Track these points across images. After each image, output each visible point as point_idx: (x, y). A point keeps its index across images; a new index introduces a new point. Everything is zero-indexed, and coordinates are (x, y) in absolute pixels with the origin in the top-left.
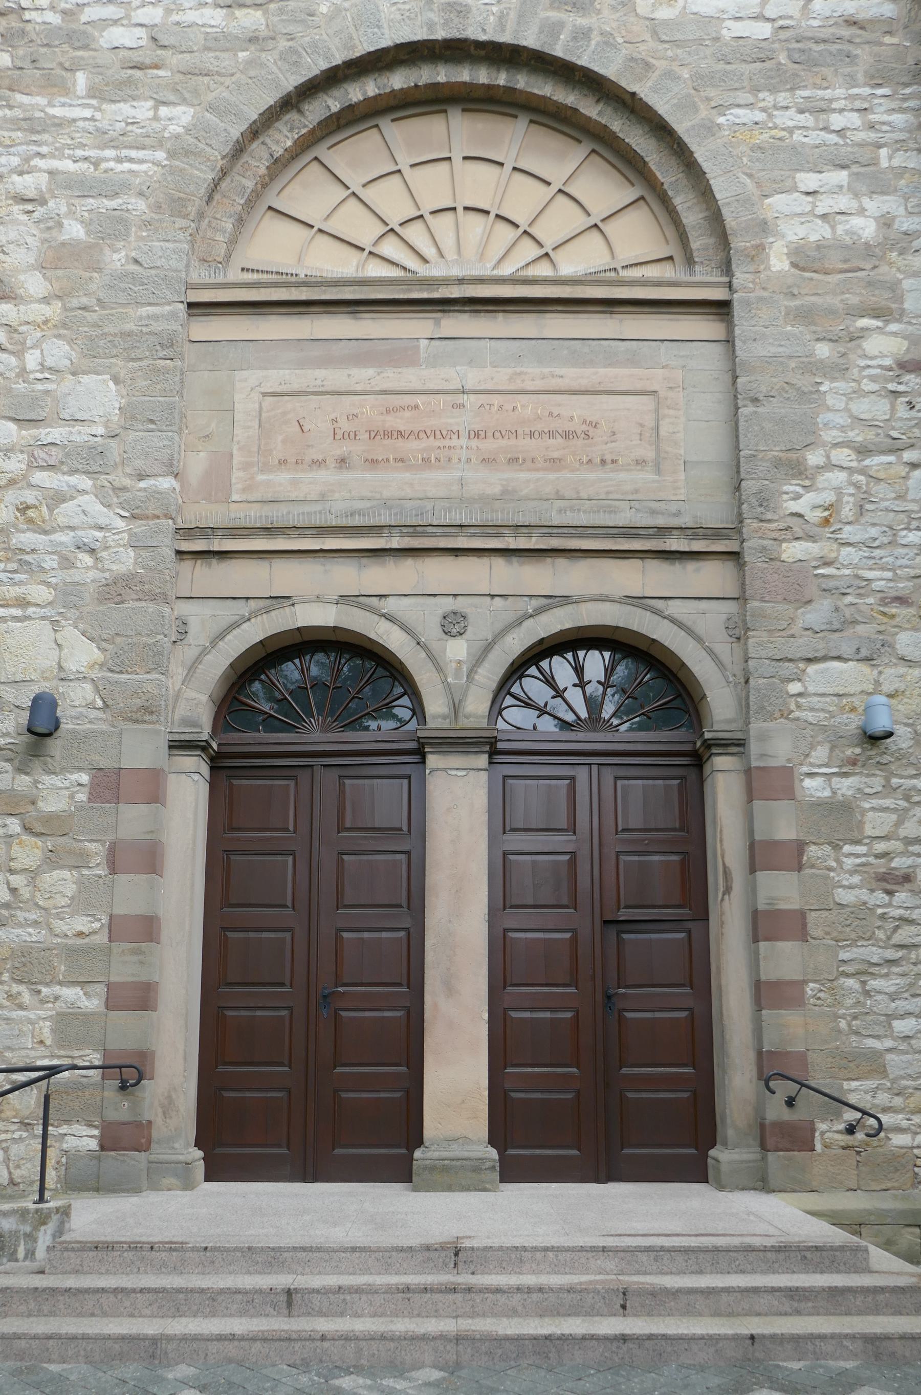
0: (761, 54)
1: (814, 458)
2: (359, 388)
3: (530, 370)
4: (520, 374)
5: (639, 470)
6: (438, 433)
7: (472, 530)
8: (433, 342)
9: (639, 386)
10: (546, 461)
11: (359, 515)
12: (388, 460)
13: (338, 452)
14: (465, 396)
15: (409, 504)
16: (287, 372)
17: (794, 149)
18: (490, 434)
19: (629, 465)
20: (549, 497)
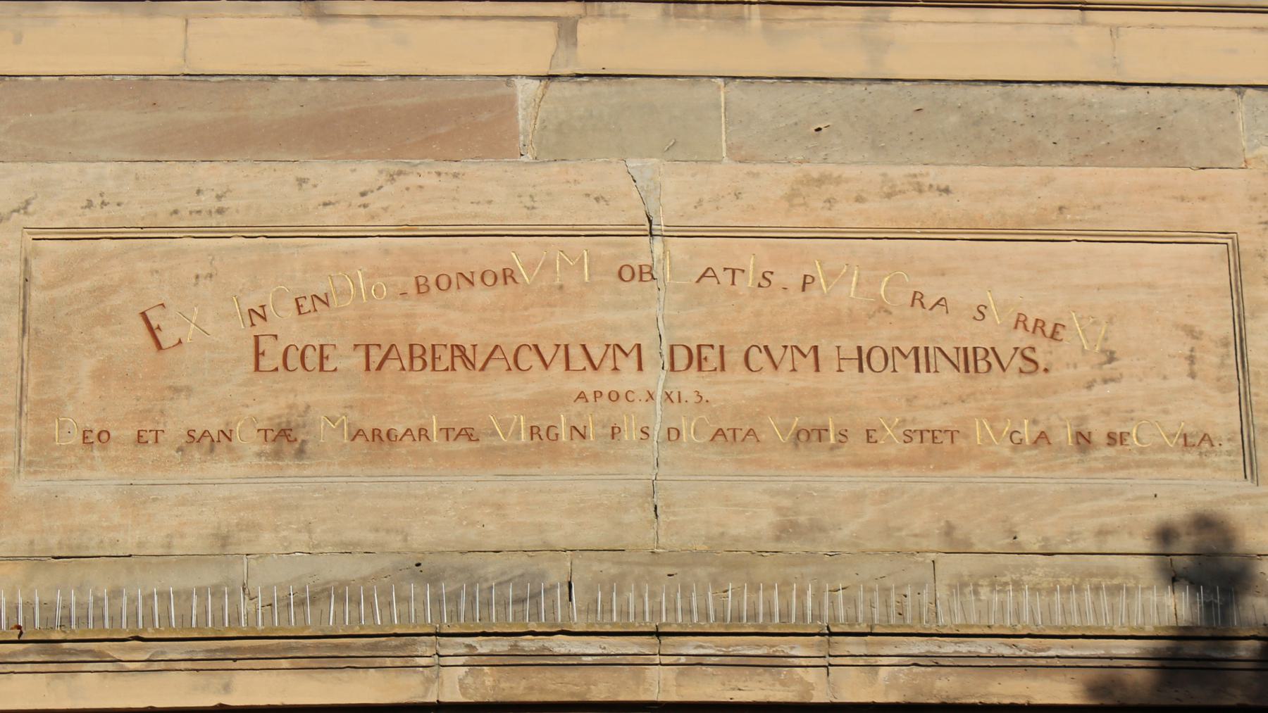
2: (332, 218)
3: (849, 171)
4: (821, 181)
5: (1191, 465)
6: (576, 352)
7: (691, 646)
8: (554, 85)
9: (1177, 216)
10: (908, 437)
11: (340, 599)
12: (423, 433)
13: (270, 403)
14: (658, 244)
15: (493, 567)
16: (110, 168)
18: (734, 357)
19: (1163, 448)
20: (925, 544)
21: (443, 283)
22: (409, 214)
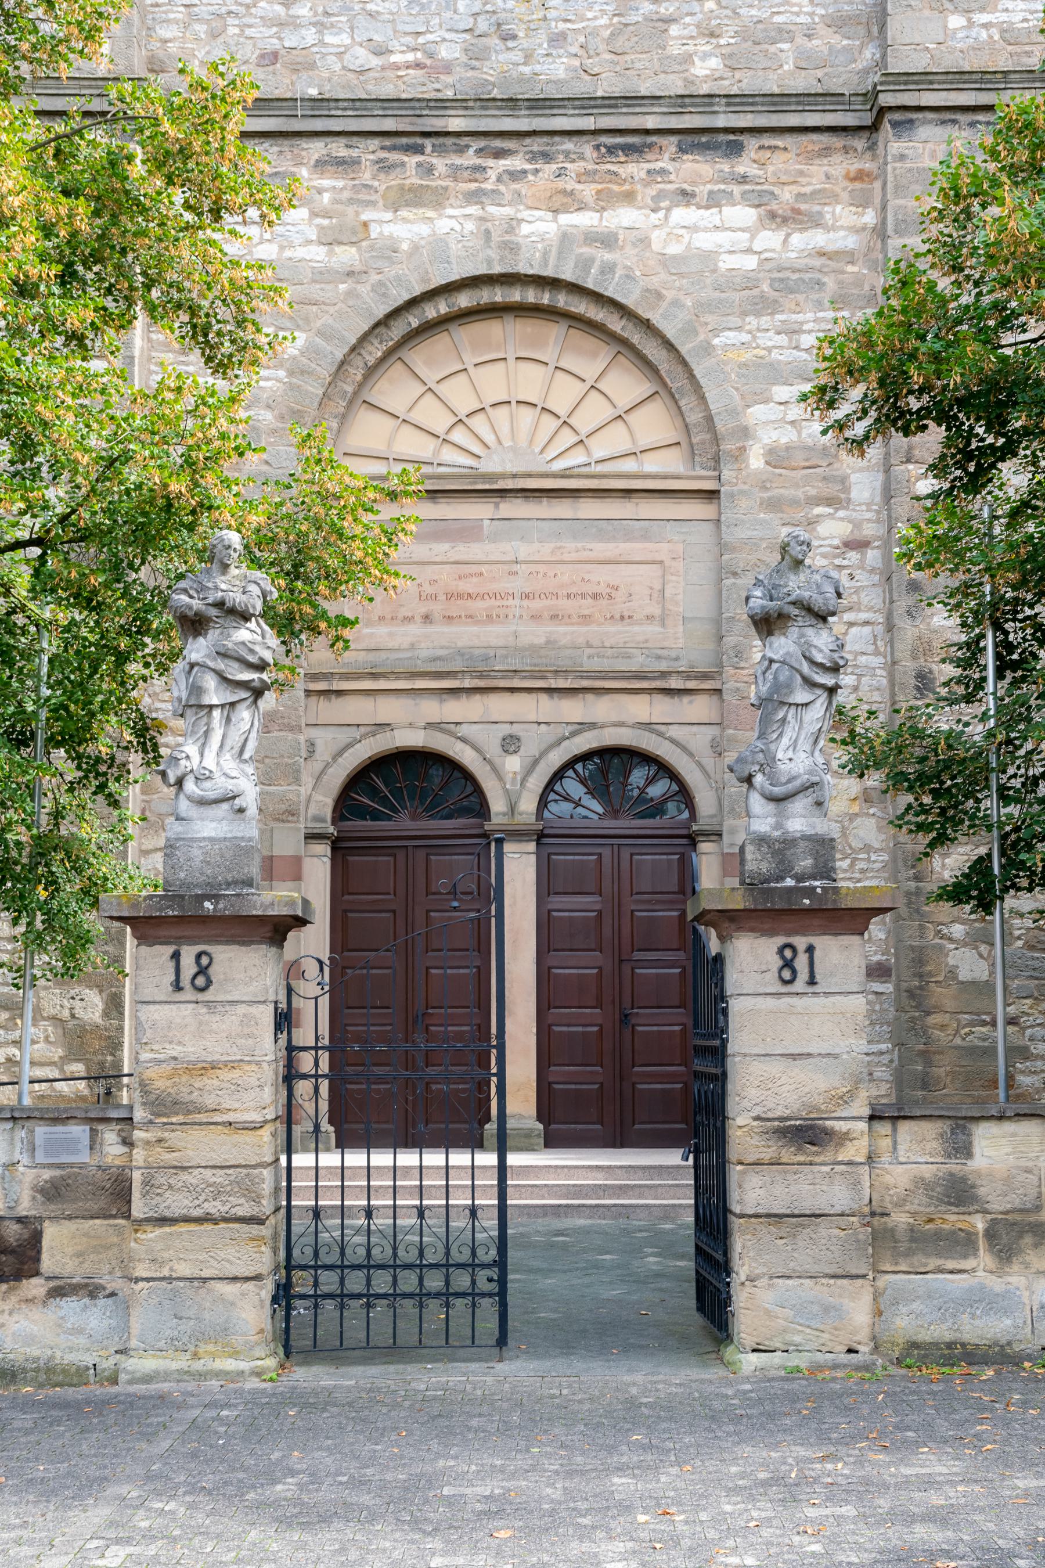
9: (649, 557)
13: (423, 610)
15: (477, 652)
21: (465, 576)
22: (457, 558)
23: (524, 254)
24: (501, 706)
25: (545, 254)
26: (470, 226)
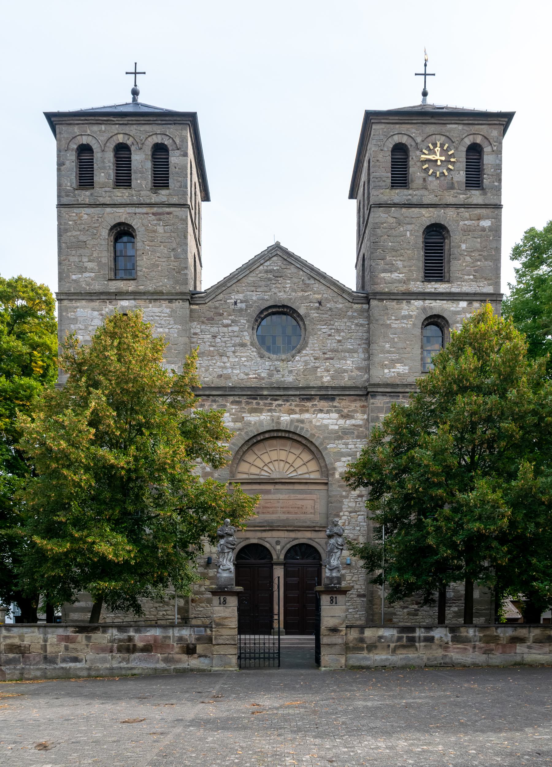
0: (336, 432)
1: (341, 514)
17: (342, 453)
23: (282, 425)
24: (276, 534)
25: (287, 425)
26: (269, 418)
